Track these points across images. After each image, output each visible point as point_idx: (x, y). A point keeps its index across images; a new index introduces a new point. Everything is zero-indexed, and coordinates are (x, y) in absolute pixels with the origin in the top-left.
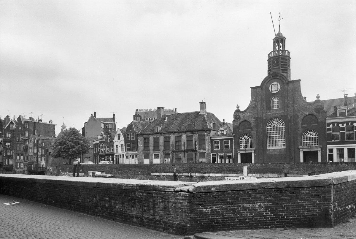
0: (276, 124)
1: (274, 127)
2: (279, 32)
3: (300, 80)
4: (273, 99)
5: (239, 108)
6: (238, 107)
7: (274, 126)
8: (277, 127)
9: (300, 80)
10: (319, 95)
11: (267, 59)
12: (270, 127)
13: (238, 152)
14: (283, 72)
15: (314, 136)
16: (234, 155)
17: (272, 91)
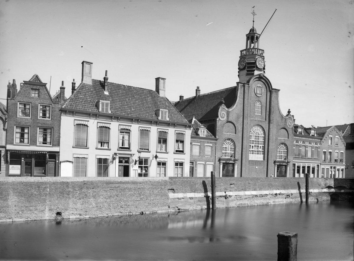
3: (279, 90)
9: (279, 90)
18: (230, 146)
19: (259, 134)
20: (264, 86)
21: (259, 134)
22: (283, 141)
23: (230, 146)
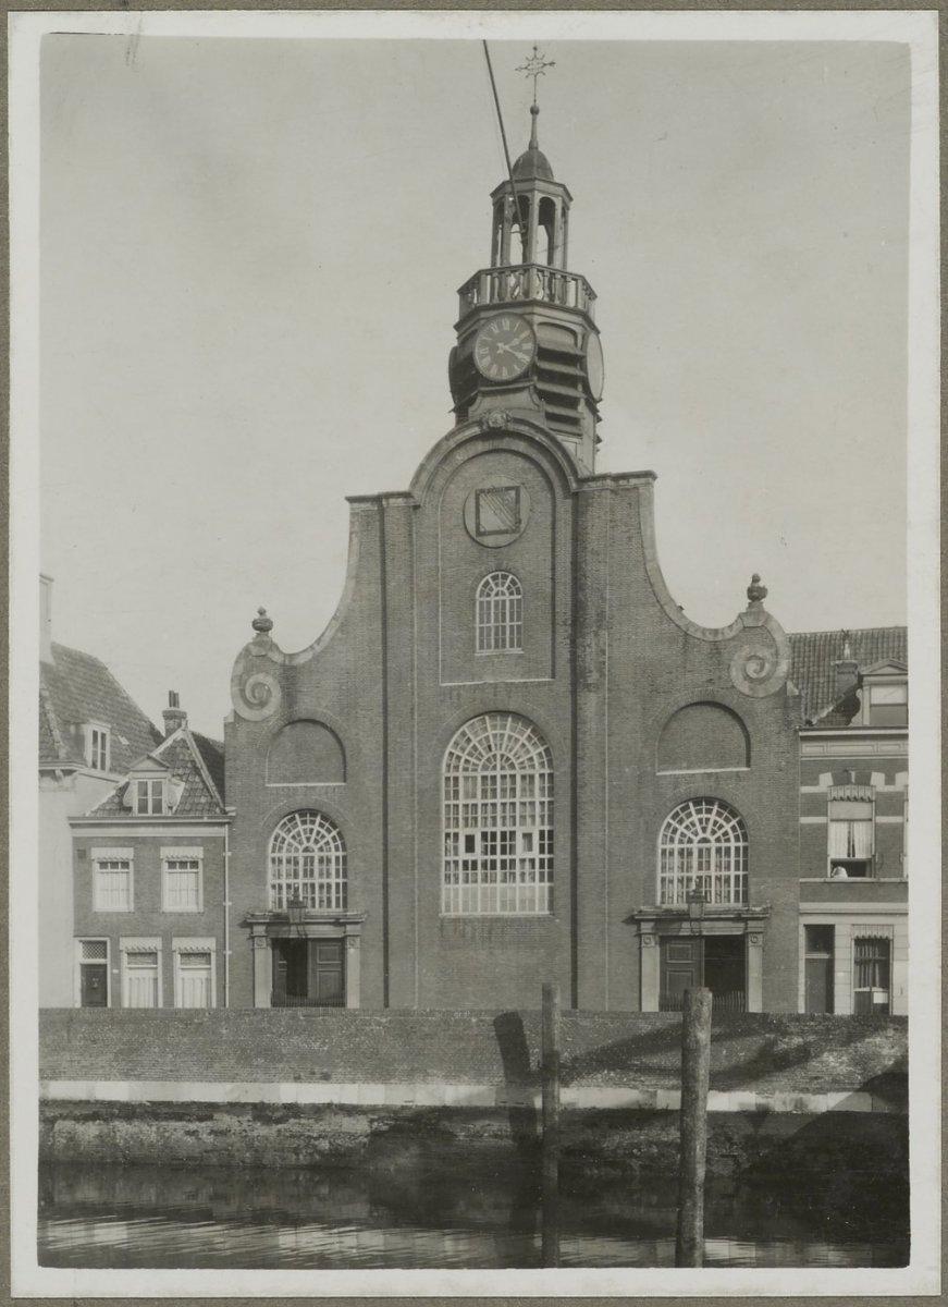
2: (533, 146)
3: (649, 475)
6: (262, 626)
7: (485, 768)
8: (508, 772)
11: (457, 319)
14: (551, 417)
15: (728, 840)
16: (228, 952)
18: (321, 849)
20: (533, 478)
21: (512, 766)
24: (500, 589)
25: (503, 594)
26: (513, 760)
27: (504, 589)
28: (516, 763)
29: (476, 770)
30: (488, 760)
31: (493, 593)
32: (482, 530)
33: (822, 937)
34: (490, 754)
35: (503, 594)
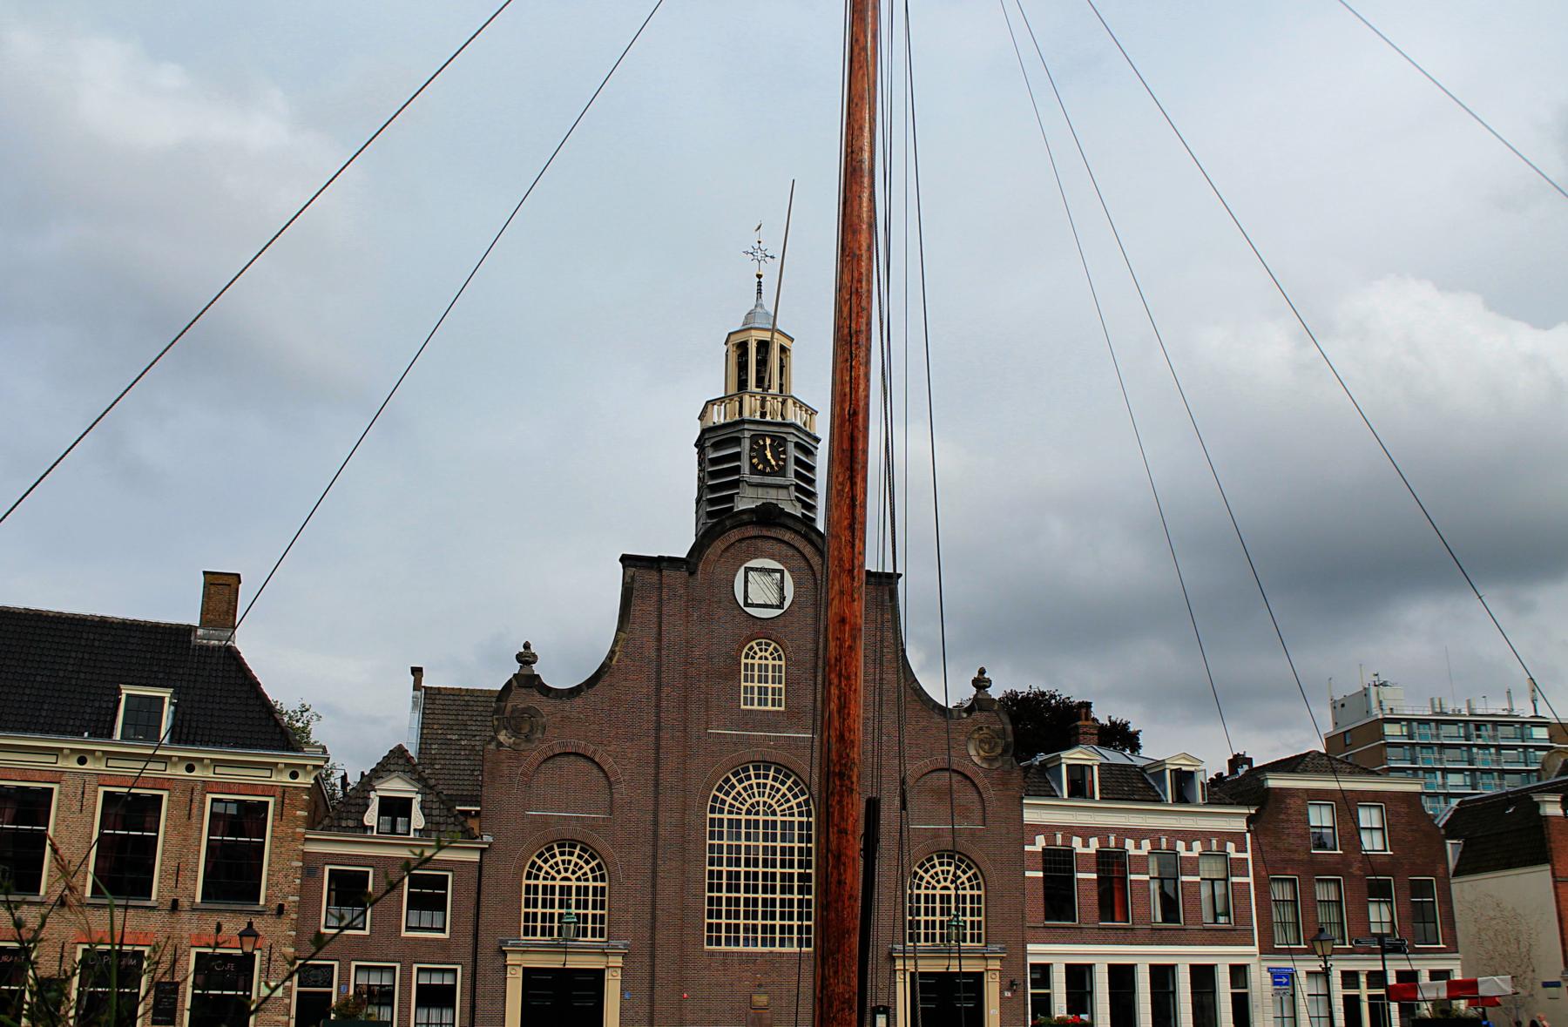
0: (762, 800)
1: (752, 817)
4: (751, 648)
5: (536, 669)
7: (748, 812)
8: (770, 818)
10: (986, 676)
12: (730, 812)
13: (511, 959)
17: (746, 604)
19: (774, 813)
21: (774, 813)
22: (946, 843)
23: (573, 877)
24: (763, 654)
25: (766, 659)
26: (775, 806)
27: (767, 654)
28: (778, 810)
29: (740, 814)
30: (752, 805)
31: (757, 657)
32: (749, 601)
33: (1042, 973)
34: (754, 800)
35: (766, 659)
